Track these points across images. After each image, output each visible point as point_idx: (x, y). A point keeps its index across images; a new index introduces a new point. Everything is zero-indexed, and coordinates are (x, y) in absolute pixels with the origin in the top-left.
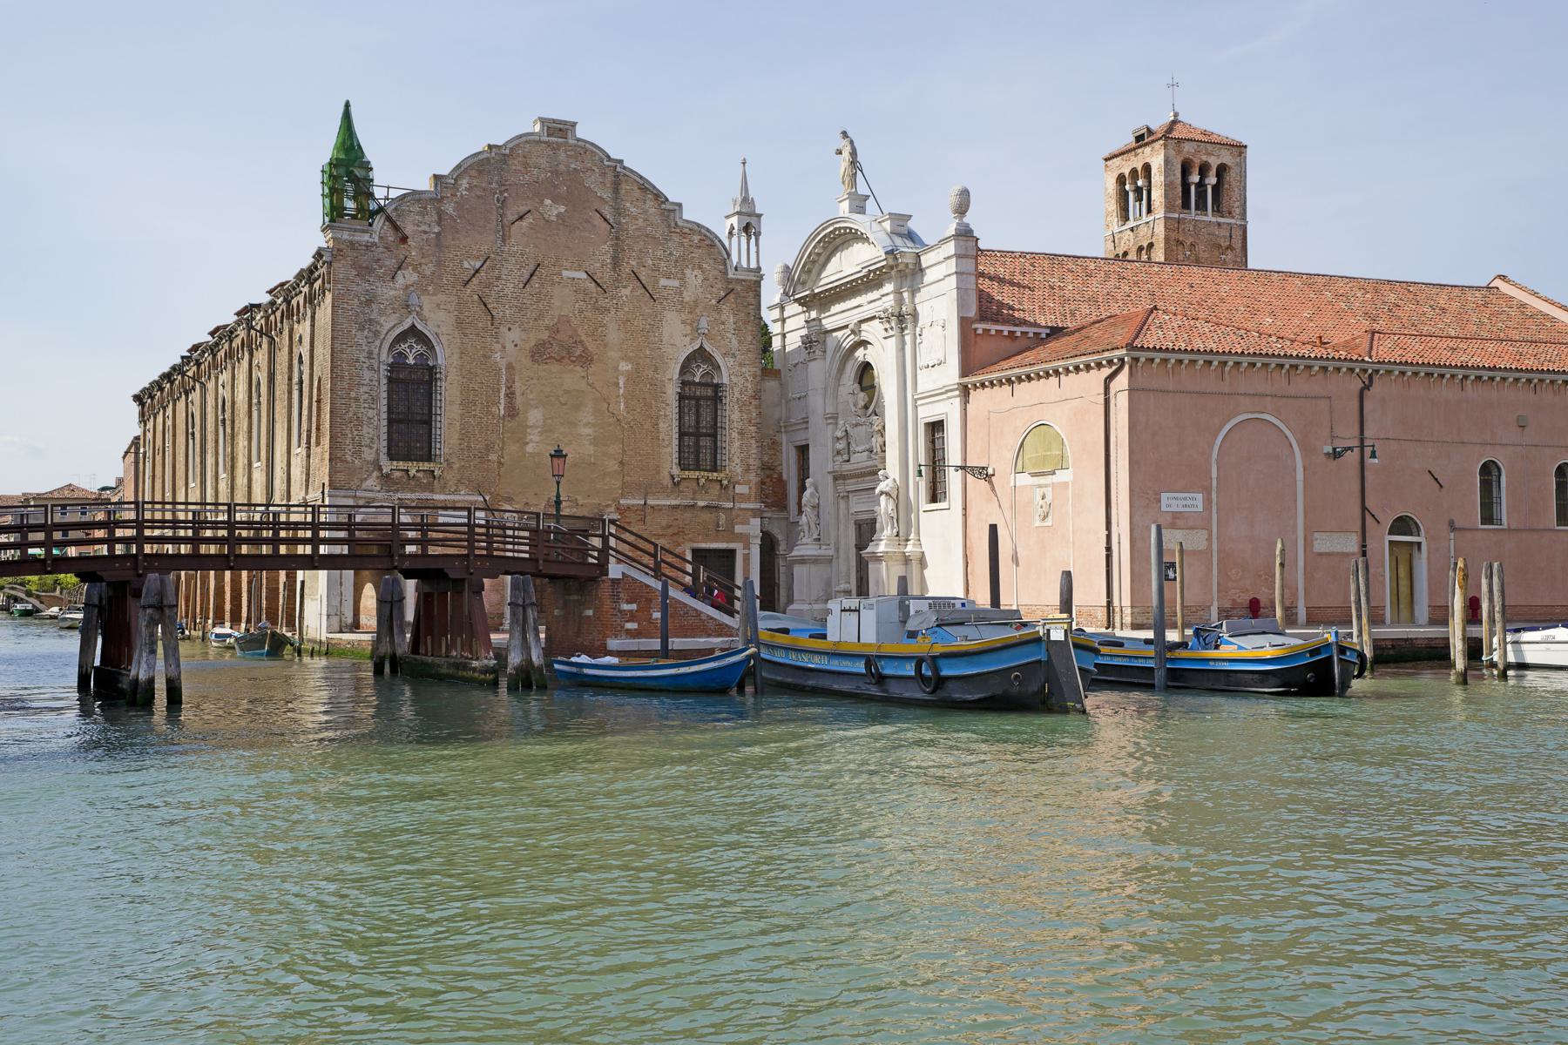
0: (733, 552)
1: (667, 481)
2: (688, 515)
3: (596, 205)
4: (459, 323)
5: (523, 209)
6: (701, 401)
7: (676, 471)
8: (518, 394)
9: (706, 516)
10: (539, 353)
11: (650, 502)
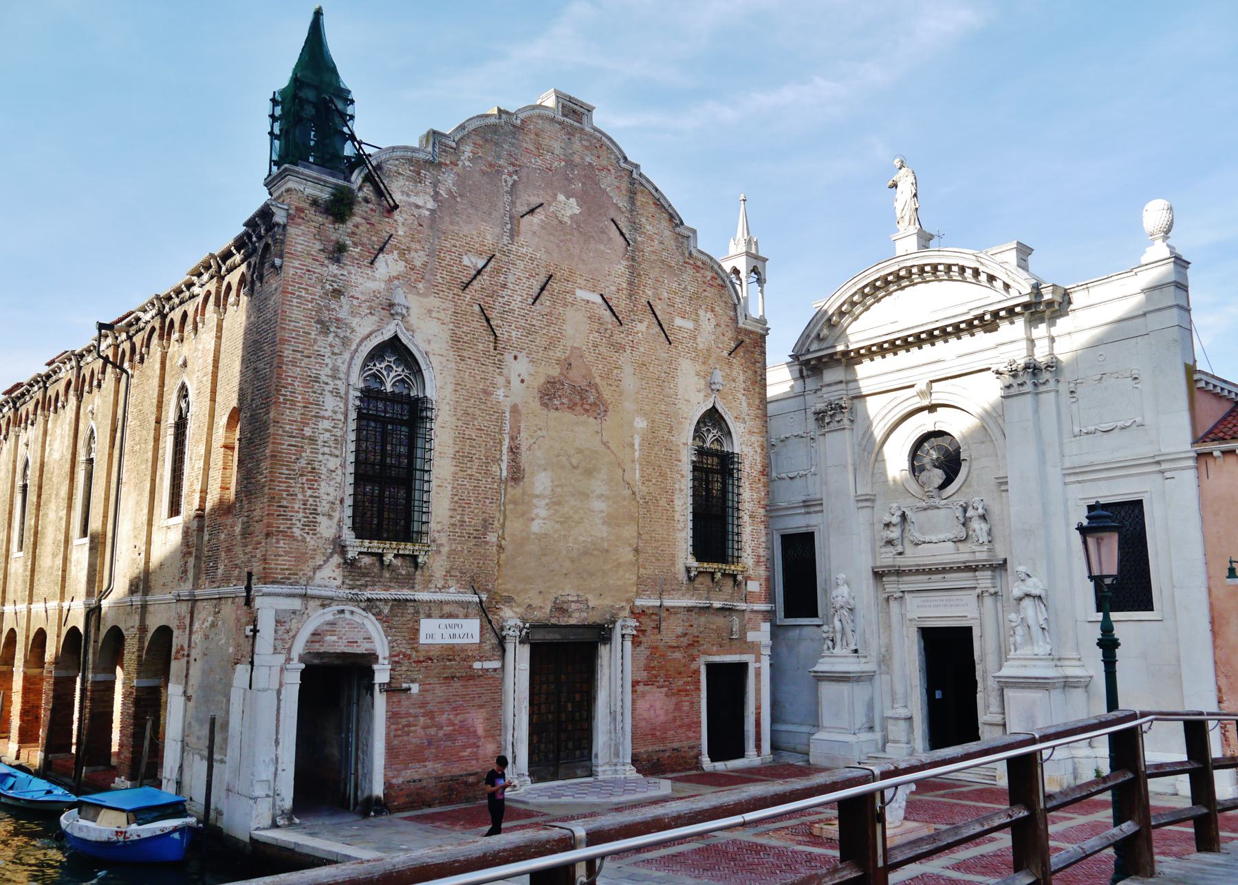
0: (743, 667)
1: (682, 576)
2: (703, 619)
3: (613, 213)
4: (456, 340)
5: (535, 201)
6: (714, 474)
8: (523, 448)
9: (720, 621)
10: (550, 393)
11: (668, 603)
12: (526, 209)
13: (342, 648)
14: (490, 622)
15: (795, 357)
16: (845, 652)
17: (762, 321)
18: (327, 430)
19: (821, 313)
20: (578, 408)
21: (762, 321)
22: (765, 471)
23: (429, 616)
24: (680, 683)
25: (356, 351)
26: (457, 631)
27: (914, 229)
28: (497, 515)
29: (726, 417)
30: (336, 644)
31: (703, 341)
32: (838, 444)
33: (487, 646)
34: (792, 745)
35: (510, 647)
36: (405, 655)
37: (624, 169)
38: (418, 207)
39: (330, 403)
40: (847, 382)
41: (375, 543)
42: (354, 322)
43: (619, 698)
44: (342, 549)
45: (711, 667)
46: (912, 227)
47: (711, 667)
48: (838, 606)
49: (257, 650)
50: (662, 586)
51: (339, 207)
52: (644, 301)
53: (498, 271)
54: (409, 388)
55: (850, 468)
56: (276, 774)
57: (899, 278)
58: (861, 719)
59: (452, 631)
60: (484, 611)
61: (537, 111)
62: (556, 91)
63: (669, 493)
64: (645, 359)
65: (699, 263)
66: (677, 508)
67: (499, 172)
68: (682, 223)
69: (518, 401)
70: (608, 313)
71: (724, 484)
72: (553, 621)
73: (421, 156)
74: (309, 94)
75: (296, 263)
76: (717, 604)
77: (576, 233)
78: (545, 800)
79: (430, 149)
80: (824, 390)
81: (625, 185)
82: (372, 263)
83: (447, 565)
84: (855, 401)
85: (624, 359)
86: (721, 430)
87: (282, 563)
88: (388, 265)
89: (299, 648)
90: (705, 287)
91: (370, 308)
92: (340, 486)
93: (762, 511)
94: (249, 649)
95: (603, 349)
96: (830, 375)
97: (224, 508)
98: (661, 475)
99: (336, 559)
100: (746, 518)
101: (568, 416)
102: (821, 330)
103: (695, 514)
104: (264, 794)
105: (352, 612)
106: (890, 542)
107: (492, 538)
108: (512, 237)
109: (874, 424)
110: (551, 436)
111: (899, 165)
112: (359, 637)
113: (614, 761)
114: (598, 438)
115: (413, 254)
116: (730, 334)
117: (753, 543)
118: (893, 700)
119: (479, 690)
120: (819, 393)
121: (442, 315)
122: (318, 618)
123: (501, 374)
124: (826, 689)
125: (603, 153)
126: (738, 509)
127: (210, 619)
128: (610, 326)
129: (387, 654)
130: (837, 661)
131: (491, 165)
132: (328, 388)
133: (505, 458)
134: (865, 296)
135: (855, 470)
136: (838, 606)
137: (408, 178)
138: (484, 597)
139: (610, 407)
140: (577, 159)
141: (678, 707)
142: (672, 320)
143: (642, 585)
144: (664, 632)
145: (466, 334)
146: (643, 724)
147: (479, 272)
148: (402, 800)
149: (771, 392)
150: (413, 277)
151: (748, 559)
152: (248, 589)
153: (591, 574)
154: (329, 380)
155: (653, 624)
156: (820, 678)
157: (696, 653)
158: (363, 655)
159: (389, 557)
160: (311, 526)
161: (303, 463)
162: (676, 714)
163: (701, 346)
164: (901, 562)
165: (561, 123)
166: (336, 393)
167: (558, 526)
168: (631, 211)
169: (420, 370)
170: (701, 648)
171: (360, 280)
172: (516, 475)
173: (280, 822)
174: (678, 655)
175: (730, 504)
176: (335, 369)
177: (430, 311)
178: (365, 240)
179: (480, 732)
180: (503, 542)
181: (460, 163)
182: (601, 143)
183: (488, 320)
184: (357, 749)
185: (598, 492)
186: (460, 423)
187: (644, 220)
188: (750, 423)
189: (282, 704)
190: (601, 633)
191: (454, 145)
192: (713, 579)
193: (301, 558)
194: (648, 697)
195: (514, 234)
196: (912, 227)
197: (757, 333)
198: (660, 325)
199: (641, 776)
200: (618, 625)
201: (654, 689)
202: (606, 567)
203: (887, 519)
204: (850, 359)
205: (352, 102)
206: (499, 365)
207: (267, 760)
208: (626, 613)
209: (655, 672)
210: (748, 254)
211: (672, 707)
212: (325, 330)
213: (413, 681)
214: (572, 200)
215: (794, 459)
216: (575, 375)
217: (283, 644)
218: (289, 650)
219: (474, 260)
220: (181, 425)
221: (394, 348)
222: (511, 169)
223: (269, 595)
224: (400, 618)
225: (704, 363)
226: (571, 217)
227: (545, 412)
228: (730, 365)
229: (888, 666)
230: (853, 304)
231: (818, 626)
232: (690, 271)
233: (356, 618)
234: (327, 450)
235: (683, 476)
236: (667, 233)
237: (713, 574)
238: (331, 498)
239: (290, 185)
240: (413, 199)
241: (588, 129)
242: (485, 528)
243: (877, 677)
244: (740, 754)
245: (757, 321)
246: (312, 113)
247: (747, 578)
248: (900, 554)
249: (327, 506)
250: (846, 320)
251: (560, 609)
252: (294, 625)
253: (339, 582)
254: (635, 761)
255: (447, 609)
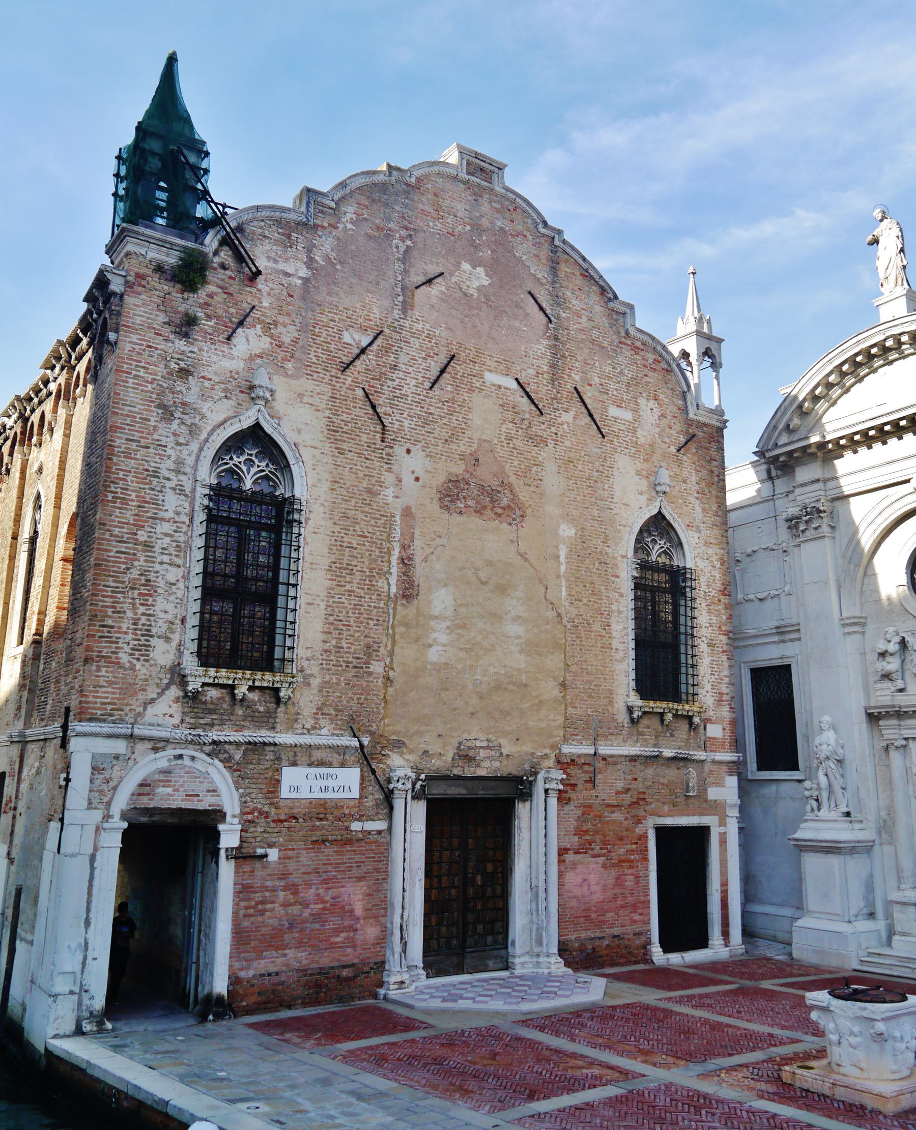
0: (704, 831)
2: (650, 772)
3: (530, 285)
4: (333, 430)
5: (433, 270)
6: (662, 595)
7: (635, 700)
8: (418, 560)
9: (672, 773)
10: (451, 494)
11: (604, 750)
12: (423, 279)
13: (178, 802)
14: (373, 772)
15: (760, 453)
16: (833, 815)
17: (719, 412)
18: (166, 535)
19: (789, 400)
20: (488, 512)
21: (719, 412)
22: (728, 589)
23: (294, 764)
24: (622, 851)
25: (206, 440)
26: (330, 783)
27: (902, 290)
28: (384, 640)
29: (675, 525)
30: (170, 797)
31: (644, 435)
32: (816, 556)
33: (369, 802)
34: (771, 932)
35: (399, 804)
36: (261, 813)
37: (544, 235)
38: (287, 275)
39: (172, 502)
40: (825, 481)
41: (223, 672)
42: (205, 407)
43: (542, 869)
44: (182, 680)
45: (662, 833)
46: (899, 288)
47: (662, 833)
48: (822, 756)
49: (67, 805)
50: (598, 729)
51: (190, 274)
52: (570, 387)
53: (387, 350)
54: (275, 487)
55: (833, 586)
56: (84, 964)
57: (886, 350)
58: (857, 903)
59: (323, 783)
60: (366, 759)
61: (436, 169)
62: (458, 146)
63: (605, 616)
64: (572, 455)
65: (638, 344)
66: (614, 634)
67: (389, 236)
68: (616, 297)
69: (411, 502)
70: (525, 400)
71: (676, 606)
72: (456, 771)
73: (293, 216)
74: (154, 145)
75: (134, 338)
76: (668, 753)
77: (484, 307)
78: (437, 1004)
79: (303, 209)
80: (798, 491)
81: (545, 252)
82: (229, 338)
83: (318, 700)
84: (837, 503)
85: (546, 454)
86: (670, 540)
87: (103, 695)
88: (250, 341)
89: (121, 802)
90: (646, 371)
91: (226, 390)
92: (181, 602)
93: (724, 638)
94: (61, 802)
95: (519, 443)
96: (803, 474)
97: (58, 631)
98: (593, 593)
99: (175, 691)
100: (703, 647)
101: (475, 522)
102: (791, 419)
103: (640, 644)
104: (67, 990)
105: (193, 758)
106: (887, 676)
107: (377, 668)
108: (404, 311)
109: (861, 531)
110: (452, 547)
111: (879, 216)
112: (201, 788)
113: (536, 950)
114: (513, 548)
115: (280, 329)
116: (678, 427)
117: (714, 679)
118: (899, 880)
119: (357, 858)
120: (791, 497)
121: (316, 400)
122: (148, 764)
123: (389, 470)
124: (812, 863)
125: (518, 216)
126: (693, 636)
127: (37, 764)
128: (527, 416)
129: (237, 811)
130: (824, 826)
131: (378, 228)
132: (169, 484)
133: (394, 570)
134: (843, 375)
135: (839, 588)
136: (822, 756)
137: (276, 242)
138: (366, 741)
139: (528, 511)
140: (485, 223)
141: (619, 881)
142: (606, 409)
143: (571, 729)
144: (600, 787)
145: (347, 423)
146: (574, 903)
147: (363, 351)
148: (253, 999)
149: (732, 499)
150: (281, 355)
151: (707, 696)
152: (65, 727)
153: (506, 714)
154: (172, 475)
155: (586, 777)
156: (804, 847)
157: (641, 813)
158: (206, 812)
159: (242, 690)
160: (142, 650)
161: (135, 573)
162: (618, 891)
163: (642, 440)
164: (901, 700)
165: (466, 183)
166: (179, 490)
167: (462, 654)
168: (553, 283)
169: (288, 465)
170: (648, 808)
171: (214, 358)
172: (409, 591)
173: (87, 1027)
174: (618, 816)
175: (682, 629)
176: (180, 462)
177: (301, 395)
178: (220, 312)
179: (359, 911)
180: (391, 673)
181: (341, 226)
182: (516, 206)
183: (374, 407)
184: (200, 931)
185: (513, 613)
186: (337, 529)
187: (569, 293)
188: (705, 532)
189: (96, 873)
190: (518, 787)
191: (333, 205)
192: (662, 721)
193: (129, 689)
194: (580, 868)
195: (406, 307)
196: (899, 288)
197: (713, 426)
198: (591, 415)
199: (570, 971)
200: (540, 777)
201: (586, 858)
202: (525, 705)
203: (882, 646)
204: (829, 452)
205: (207, 154)
206: (388, 460)
207: (74, 945)
208: (551, 762)
209: (588, 838)
210: (699, 333)
211: (611, 882)
212: (168, 414)
213: (270, 846)
214: (480, 270)
215: (762, 577)
216: (485, 474)
217: (100, 797)
218: (109, 804)
219: (357, 337)
220: (33, 540)
221: (255, 438)
222: (404, 233)
223: (85, 735)
224: (257, 765)
225: (646, 460)
226: (479, 289)
227: (446, 516)
228: (680, 463)
229: (891, 835)
230: (830, 386)
231: (800, 781)
232: (627, 352)
233: (198, 765)
234: (166, 558)
235: (621, 595)
236: (598, 308)
237: (662, 715)
238: (169, 617)
239: (130, 248)
240: (281, 266)
241: (498, 189)
242: (369, 655)
243: (877, 848)
244: (702, 942)
245: (712, 411)
246: (162, 166)
247: (706, 721)
248: (901, 690)
249: (164, 627)
250: (821, 406)
251: (465, 756)
252: (116, 773)
253: (176, 720)
254: (563, 950)
255: (317, 755)
